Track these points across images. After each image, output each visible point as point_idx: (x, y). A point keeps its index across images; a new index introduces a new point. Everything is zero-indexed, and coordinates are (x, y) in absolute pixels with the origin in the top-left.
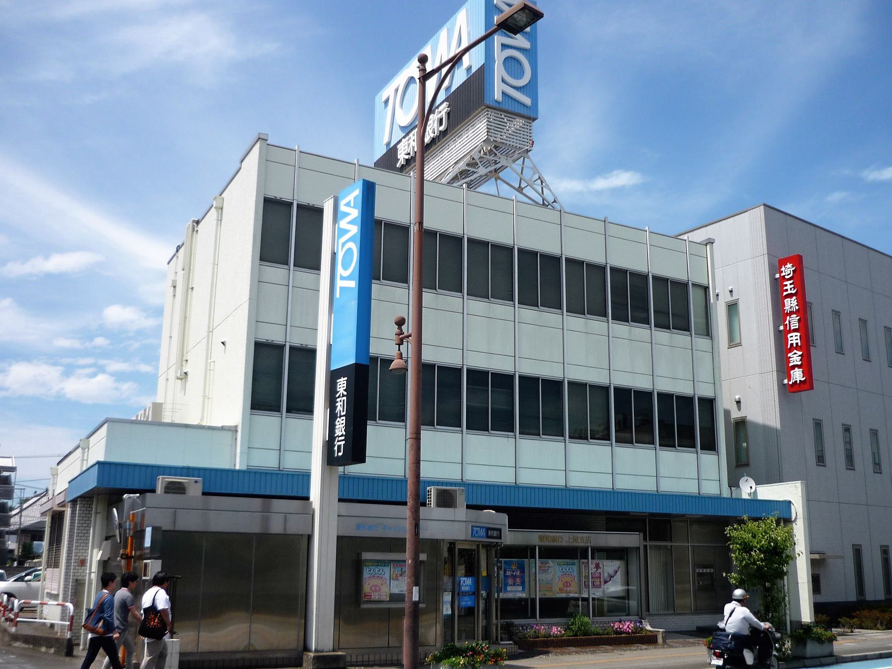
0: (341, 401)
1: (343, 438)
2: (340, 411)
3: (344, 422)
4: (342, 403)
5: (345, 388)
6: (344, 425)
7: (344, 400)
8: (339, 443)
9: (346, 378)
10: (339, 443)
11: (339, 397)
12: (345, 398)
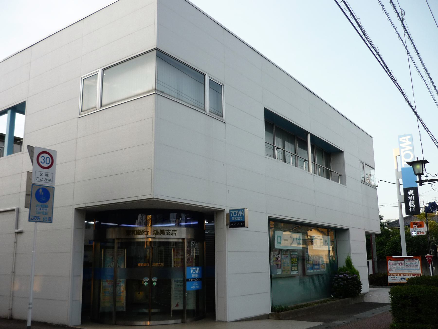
0: (411, 197)
1: (414, 207)
2: (411, 200)
3: (414, 202)
4: (412, 197)
5: (413, 193)
6: (414, 203)
7: (413, 197)
8: (412, 208)
9: (413, 191)
10: (412, 208)
11: (410, 195)
12: (413, 196)
